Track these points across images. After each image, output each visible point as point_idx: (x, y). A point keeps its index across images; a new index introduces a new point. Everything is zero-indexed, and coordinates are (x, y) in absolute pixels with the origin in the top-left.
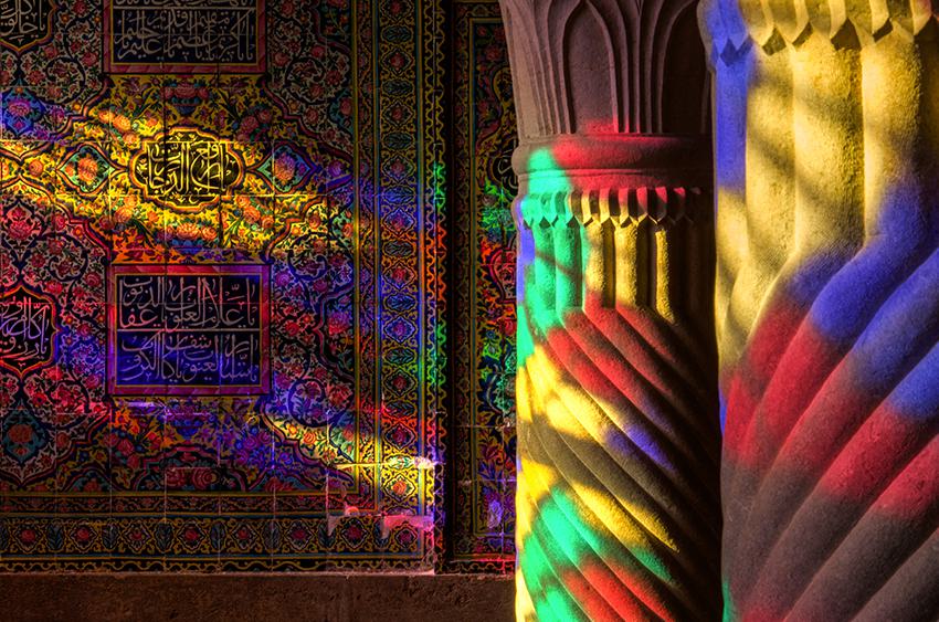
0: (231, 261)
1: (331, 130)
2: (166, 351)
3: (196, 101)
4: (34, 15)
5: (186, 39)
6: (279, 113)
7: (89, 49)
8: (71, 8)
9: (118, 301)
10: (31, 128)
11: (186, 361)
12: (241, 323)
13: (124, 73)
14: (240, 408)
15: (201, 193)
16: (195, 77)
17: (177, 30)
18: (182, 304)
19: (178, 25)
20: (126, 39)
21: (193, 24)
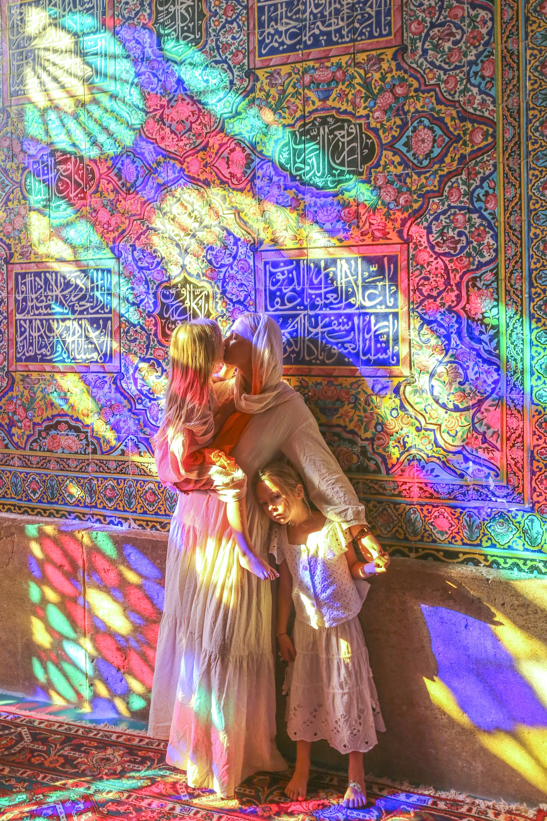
0: (369, 241)
1: (473, 95)
2: (309, 333)
3: (333, 85)
4: (191, 25)
5: (323, 23)
6: (416, 85)
7: (237, 49)
8: (221, 12)
9: (266, 286)
10: (190, 130)
11: (328, 342)
12: (380, 303)
13: (268, 67)
14: (381, 390)
15: (339, 175)
16: (332, 60)
17: (315, 15)
18: (323, 286)
19: (315, 11)
20: (269, 34)
21: (330, 5)
